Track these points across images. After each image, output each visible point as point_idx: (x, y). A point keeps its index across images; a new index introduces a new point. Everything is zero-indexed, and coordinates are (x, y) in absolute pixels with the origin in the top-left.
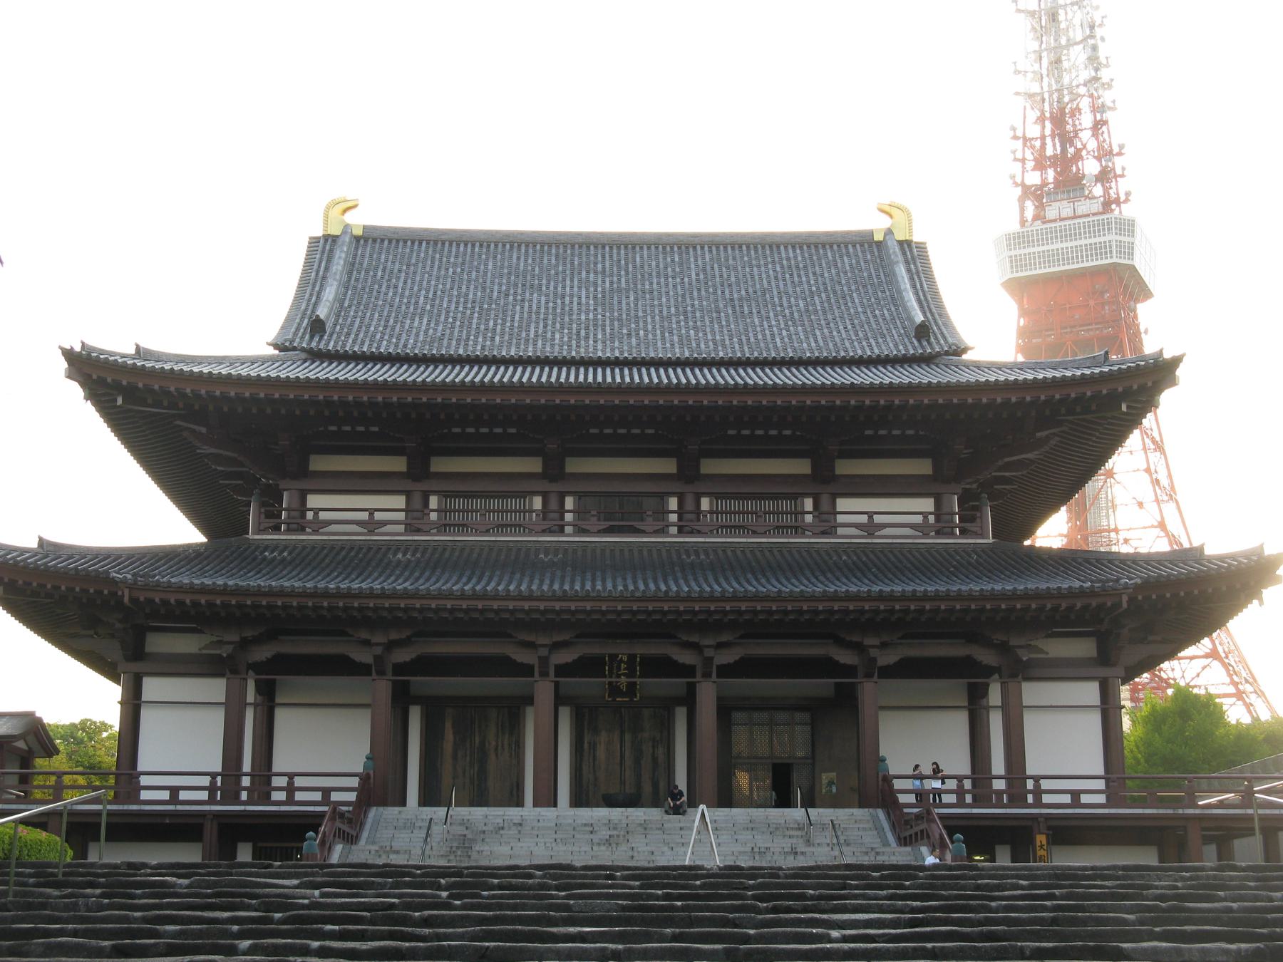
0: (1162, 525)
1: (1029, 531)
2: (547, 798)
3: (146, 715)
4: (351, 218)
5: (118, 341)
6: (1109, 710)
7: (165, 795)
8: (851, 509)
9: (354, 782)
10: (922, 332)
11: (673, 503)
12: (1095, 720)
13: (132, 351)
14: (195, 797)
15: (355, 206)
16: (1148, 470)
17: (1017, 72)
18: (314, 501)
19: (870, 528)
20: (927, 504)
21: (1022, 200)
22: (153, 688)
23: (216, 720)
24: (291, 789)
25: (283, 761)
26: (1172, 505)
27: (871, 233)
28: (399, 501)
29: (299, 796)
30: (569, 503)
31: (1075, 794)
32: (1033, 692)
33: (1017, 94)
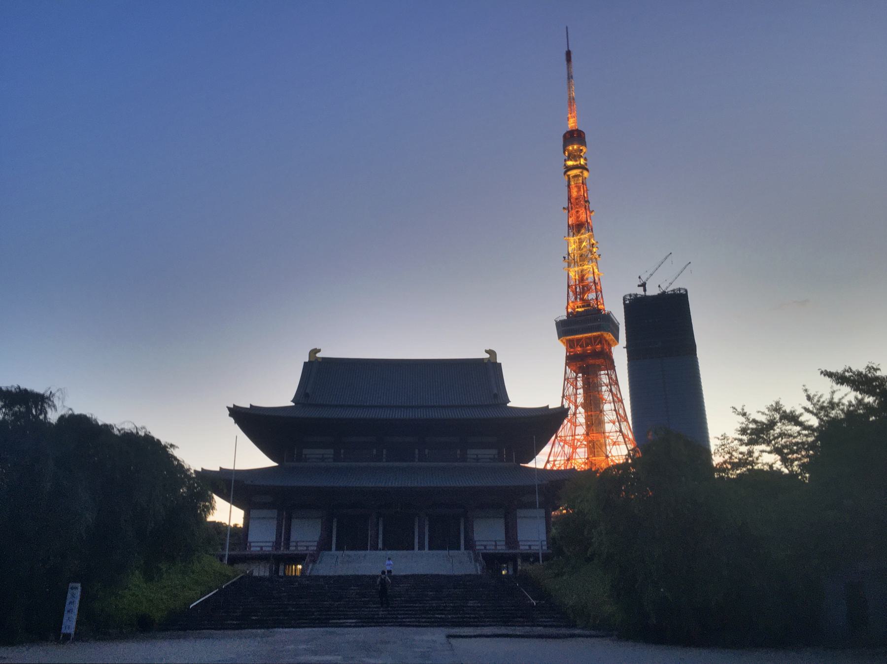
0: (621, 431)
1: (531, 457)
2: (375, 548)
3: (251, 521)
4: (319, 355)
5: (244, 403)
6: (548, 517)
7: (259, 549)
8: (472, 453)
9: (316, 543)
10: (496, 396)
11: (417, 451)
12: (544, 520)
13: (249, 406)
14: (268, 549)
15: (319, 351)
16: (615, 410)
18: (305, 451)
19: (477, 460)
20: (494, 452)
22: (254, 513)
23: (274, 523)
24: (296, 546)
25: (294, 536)
26: (625, 423)
27: (483, 359)
28: (332, 451)
29: (299, 548)
30: (385, 452)
31: (530, 546)
32: (520, 513)
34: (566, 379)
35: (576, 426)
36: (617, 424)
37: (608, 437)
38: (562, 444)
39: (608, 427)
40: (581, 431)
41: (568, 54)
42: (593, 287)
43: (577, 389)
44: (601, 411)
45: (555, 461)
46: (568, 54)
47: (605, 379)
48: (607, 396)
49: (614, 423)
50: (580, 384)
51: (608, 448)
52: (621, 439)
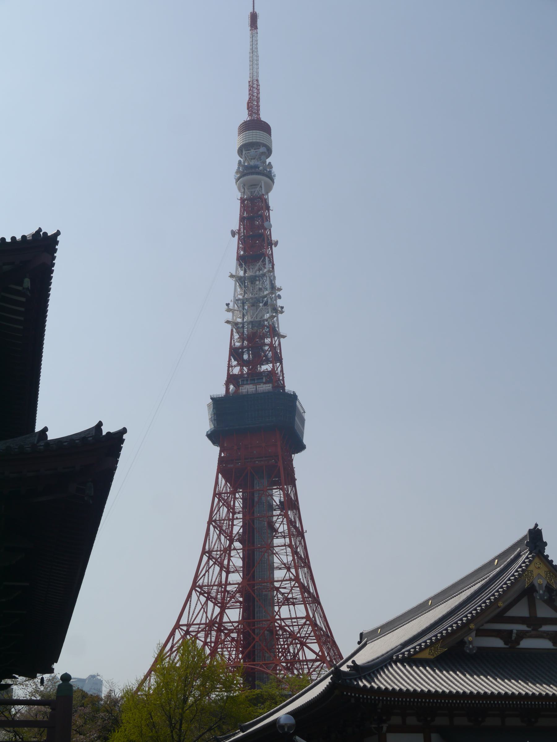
16: (290, 546)
17: (228, 310)
21: (227, 384)
33: (228, 322)
34: (217, 494)
35: (228, 572)
36: (293, 571)
37: (277, 589)
38: (203, 599)
39: (279, 574)
40: (236, 578)
41: (254, 18)
42: (270, 354)
43: (234, 513)
44: (271, 547)
45: (189, 625)
46: (254, 18)
47: (277, 496)
48: (282, 528)
49: (288, 569)
50: (238, 505)
51: (276, 608)
52: (297, 593)
